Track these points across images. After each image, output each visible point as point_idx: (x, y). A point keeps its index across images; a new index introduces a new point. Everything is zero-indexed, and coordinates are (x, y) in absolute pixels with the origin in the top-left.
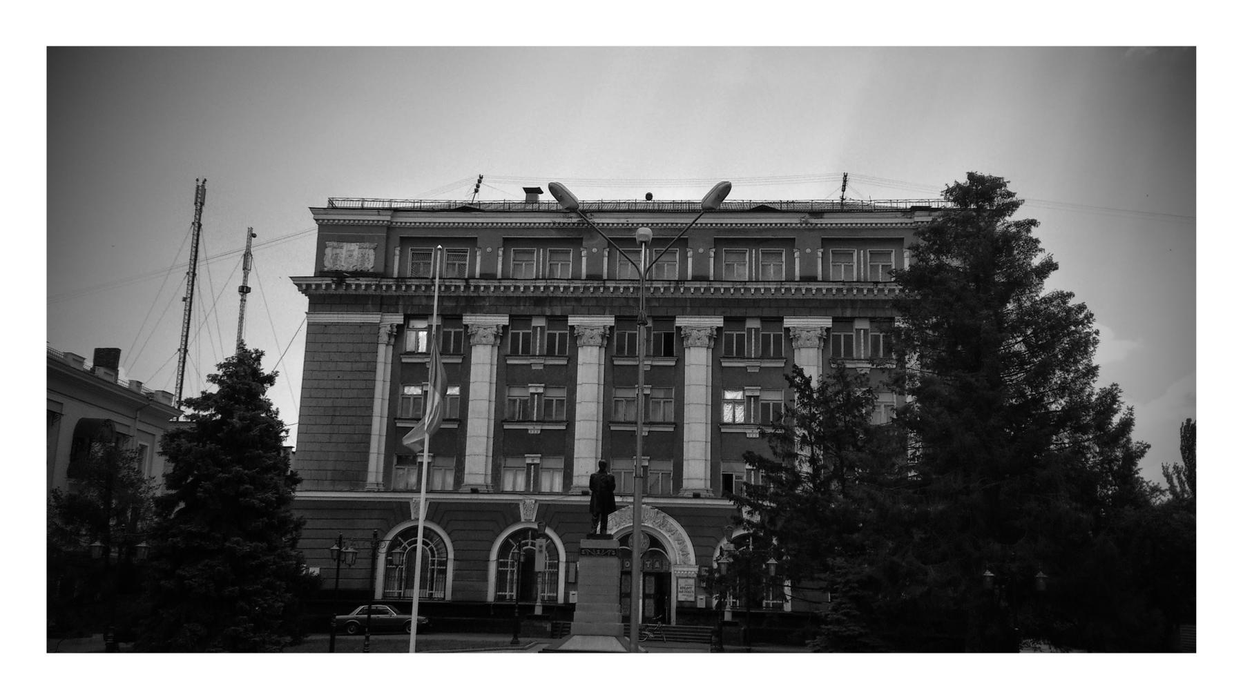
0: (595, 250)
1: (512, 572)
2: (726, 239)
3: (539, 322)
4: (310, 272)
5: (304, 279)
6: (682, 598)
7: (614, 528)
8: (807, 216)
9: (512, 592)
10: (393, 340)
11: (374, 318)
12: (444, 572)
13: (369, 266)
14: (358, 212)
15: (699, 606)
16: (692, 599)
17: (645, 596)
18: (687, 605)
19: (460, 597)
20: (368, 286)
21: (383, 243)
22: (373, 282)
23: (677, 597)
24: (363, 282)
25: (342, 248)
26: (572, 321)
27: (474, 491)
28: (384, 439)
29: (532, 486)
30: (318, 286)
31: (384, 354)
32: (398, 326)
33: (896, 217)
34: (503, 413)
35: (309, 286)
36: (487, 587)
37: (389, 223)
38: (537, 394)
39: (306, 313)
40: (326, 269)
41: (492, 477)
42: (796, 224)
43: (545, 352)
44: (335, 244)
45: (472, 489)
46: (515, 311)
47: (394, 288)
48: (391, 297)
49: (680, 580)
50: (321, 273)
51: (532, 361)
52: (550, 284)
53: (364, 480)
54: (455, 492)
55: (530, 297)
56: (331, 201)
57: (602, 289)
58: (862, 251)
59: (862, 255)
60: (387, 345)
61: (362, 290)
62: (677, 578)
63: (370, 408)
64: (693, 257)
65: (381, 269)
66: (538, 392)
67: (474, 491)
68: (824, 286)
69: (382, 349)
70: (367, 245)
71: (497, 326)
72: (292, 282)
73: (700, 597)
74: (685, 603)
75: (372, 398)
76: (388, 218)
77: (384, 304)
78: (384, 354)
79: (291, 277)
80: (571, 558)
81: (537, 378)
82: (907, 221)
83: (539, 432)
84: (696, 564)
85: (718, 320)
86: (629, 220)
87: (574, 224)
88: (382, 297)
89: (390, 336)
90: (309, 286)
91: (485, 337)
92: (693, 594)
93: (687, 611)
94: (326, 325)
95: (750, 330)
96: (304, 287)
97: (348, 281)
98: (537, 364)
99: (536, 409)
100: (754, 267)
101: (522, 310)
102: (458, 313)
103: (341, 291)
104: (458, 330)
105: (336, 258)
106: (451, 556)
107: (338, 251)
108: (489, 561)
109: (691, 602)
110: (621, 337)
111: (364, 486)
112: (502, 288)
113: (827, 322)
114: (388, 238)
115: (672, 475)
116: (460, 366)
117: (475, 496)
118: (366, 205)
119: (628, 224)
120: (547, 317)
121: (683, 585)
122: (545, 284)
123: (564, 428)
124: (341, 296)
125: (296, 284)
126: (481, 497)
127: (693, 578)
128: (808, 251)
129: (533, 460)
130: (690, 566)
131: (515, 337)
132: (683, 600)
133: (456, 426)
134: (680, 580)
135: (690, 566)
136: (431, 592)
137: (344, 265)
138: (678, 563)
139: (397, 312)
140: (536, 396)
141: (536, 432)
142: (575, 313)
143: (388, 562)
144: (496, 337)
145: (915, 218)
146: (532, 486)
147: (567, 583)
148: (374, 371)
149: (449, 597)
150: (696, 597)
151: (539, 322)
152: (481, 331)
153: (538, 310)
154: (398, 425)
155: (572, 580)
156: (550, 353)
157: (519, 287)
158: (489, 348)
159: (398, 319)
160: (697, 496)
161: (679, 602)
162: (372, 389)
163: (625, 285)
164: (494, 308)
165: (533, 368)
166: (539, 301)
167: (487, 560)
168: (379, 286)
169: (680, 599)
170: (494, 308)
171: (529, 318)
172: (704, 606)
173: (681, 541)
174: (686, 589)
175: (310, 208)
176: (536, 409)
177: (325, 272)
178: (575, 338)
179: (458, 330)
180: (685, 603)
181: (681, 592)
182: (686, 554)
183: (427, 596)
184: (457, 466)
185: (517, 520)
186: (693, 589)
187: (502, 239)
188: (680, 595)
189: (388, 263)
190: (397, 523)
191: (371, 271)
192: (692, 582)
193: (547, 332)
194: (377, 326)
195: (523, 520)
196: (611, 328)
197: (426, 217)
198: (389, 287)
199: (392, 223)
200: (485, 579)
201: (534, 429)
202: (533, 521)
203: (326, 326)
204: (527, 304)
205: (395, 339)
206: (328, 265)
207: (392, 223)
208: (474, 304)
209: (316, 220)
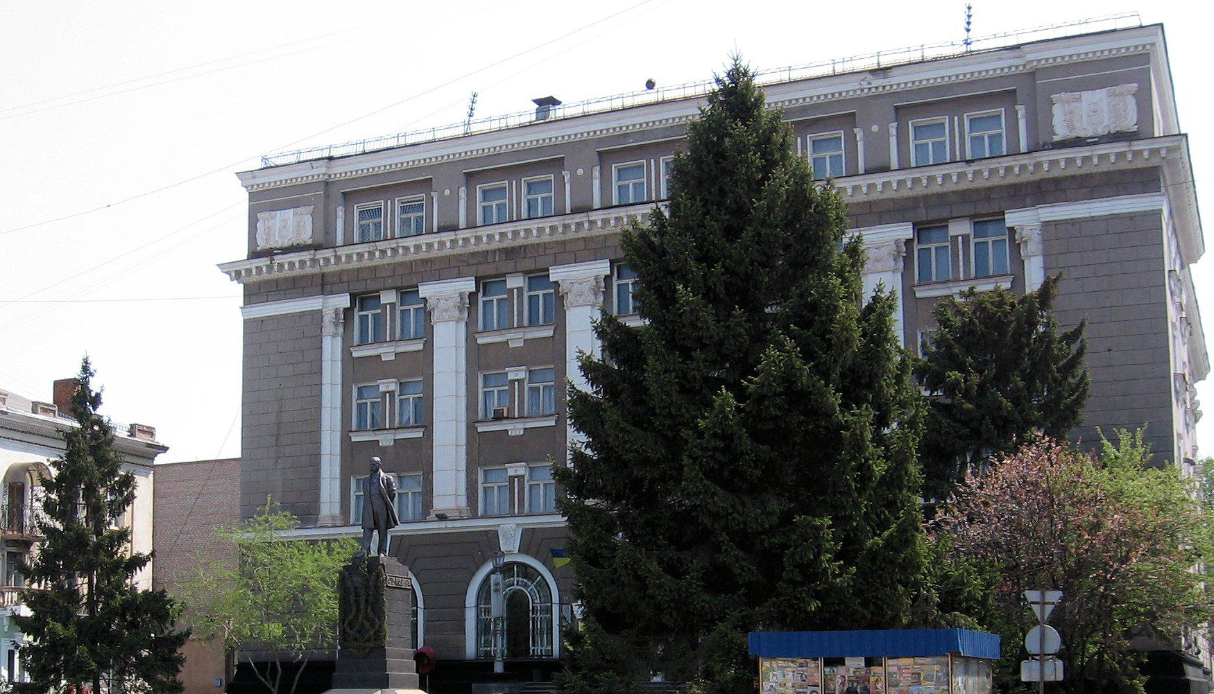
2: (922, 104)
3: (514, 282)
4: (243, 254)
5: (230, 265)
8: (869, 76)
10: (341, 330)
11: (313, 303)
13: (306, 237)
14: (463, 141)
20: (302, 263)
21: (321, 206)
22: (306, 256)
24: (295, 257)
25: (274, 217)
27: (442, 517)
28: (338, 458)
30: (249, 271)
31: (332, 348)
35: (238, 273)
37: (326, 177)
39: (241, 308)
40: (259, 249)
42: (855, 91)
43: (526, 322)
44: (266, 214)
45: (437, 516)
47: (332, 261)
48: (334, 273)
50: (254, 254)
54: (423, 520)
55: (499, 250)
56: (264, 159)
57: (586, 225)
58: (956, 118)
59: (956, 123)
60: (334, 336)
61: (298, 271)
63: (318, 420)
64: (438, 201)
65: (321, 239)
67: (442, 517)
68: (907, 176)
69: (327, 342)
70: (302, 209)
71: (461, 295)
72: (220, 270)
75: (319, 407)
76: (323, 170)
77: (323, 284)
78: (332, 348)
79: (218, 265)
81: (517, 358)
83: (522, 433)
85: (602, 266)
86: (621, 121)
88: (323, 275)
89: (336, 325)
90: (238, 273)
91: (446, 311)
94: (262, 321)
96: (233, 274)
100: (514, 199)
105: (268, 230)
107: (271, 222)
110: (363, 320)
111: (316, 520)
112: (460, 242)
113: (905, 231)
114: (327, 196)
116: (421, 354)
117: (442, 524)
118: (439, 135)
119: (621, 128)
123: (553, 423)
124: (277, 281)
125: (226, 273)
126: (450, 524)
128: (875, 128)
137: (278, 241)
141: (517, 434)
144: (461, 311)
145: (1027, 56)
148: (320, 372)
151: (514, 282)
153: (510, 266)
158: (453, 324)
159: (344, 301)
162: (318, 397)
163: (617, 215)
164: (456, 271)
166: (510, 253)
168: (314, 261)
170: (456, 271)
171: (501, 276)
175: (237, 173)
177: (259, 252)
178: (560, 299)
187: (463, 176)
189: (329, 229)
191: (310, 242)
194: (317, 315)
196: (608, 279)
197: (368, 161)
198: (327, 260)
199: (330, 175)
201: (515, 429)
202: (516, 551)
203: (262, 321)
206: (262, 244)
207: (330, 175)
209: (246, 187)
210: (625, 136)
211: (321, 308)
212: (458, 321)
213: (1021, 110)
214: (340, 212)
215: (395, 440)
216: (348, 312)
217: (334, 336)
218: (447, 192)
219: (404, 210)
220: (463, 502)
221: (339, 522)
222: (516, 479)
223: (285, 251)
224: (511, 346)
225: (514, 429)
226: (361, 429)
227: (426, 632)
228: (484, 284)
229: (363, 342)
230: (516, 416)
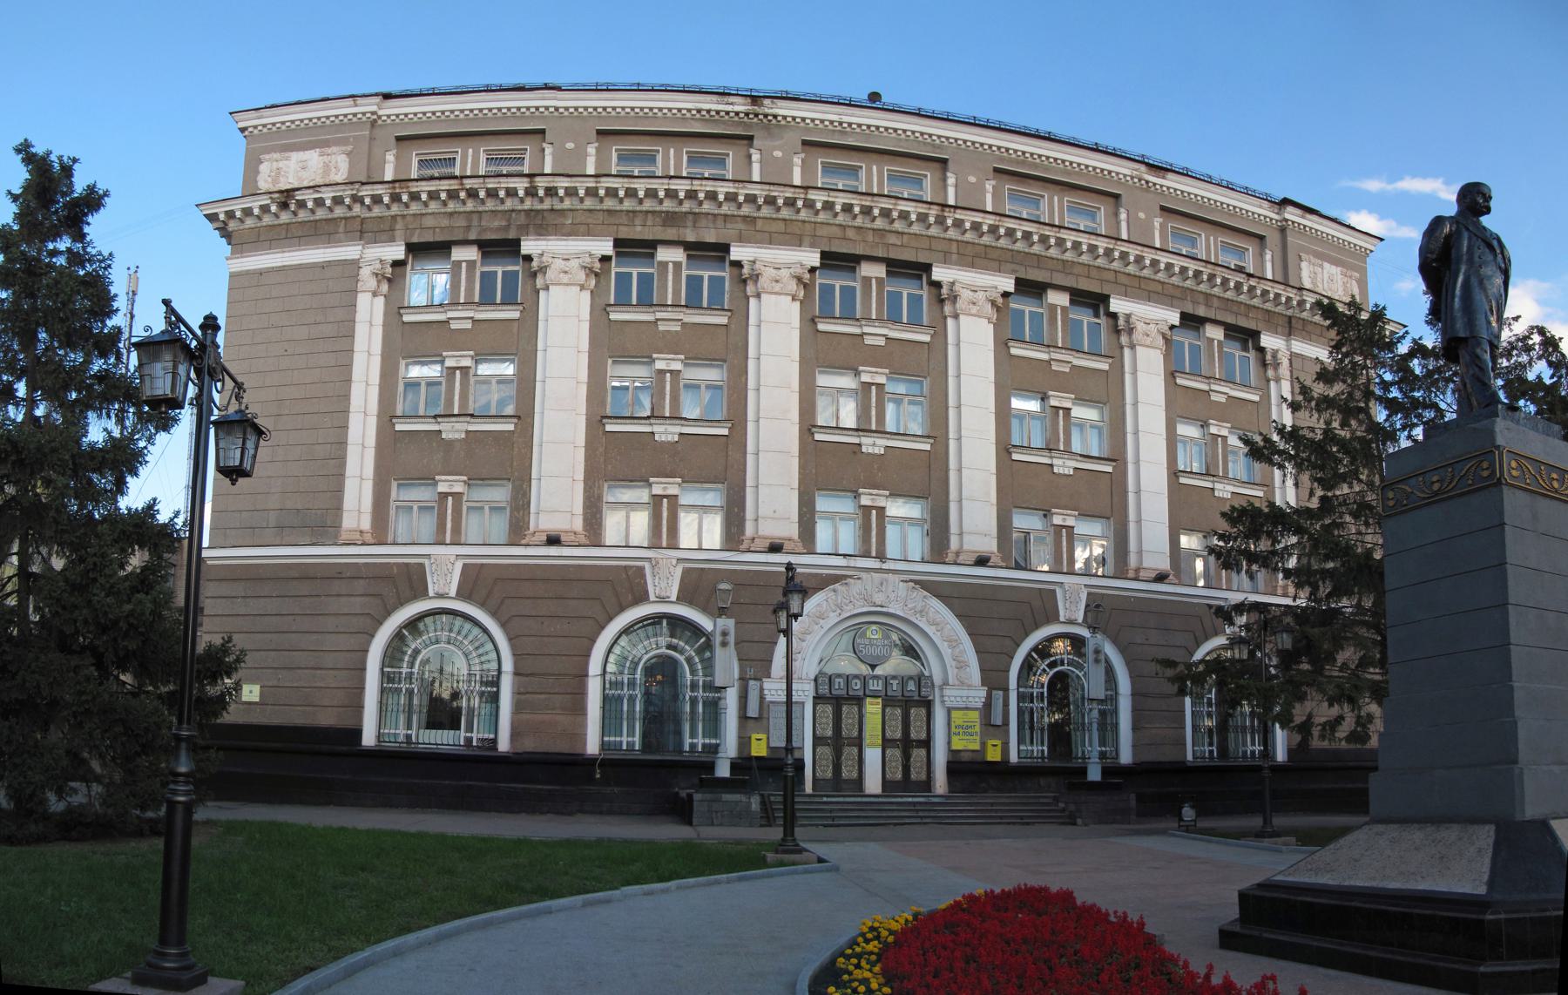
1: (632, 699)
6: (958, 744)
7: (832, 614)
9: (634, 736)
12: (495, 698)
15: (989, 758)
16: (977, 747)
17: (886, 743)
18: (965, 757)
19: (529, 745)
23: (949, 743)
26: (736, 253)
27: (553, 541)
34: (603, 403)
36: (584, 726)
38: (671, 372)
41: (585, 520)
46: (625, 233)
49: (954, 714)
51: (659, 315)
52: (698, 188)
62: (949, 711)
66: (671, 368)
67: (553, 541)
74: (962, 754)
80: (750, 673)
81: (671, 344)
84: (983, 685)
92: (978, 738)
93: (965, 770)
98: (670, 321)
99: (668, 397)
101: (639, 232)
102: (512, 235)
104: (510, 268)
106: (508, 666)
108: (587, 676)
109: (973, 751)
117: (553, 551)
120: (688, 246)
121: (959, 722)
122: (688, 188)
127: (976, 709)
129: (665, 489)
130: (970, 686)
131: (623, 279)
132: (960, 748)
133: (511, 427)
135: (970, 686)
136: (469, 735)
138: (951, 683)
141: (670, 438)
143: (386, 677)
147: (743, 717)
149: (504, 745)
150: (983, 744)
152: (558, 264)
154: (398, 427)
155: (753, 711)
160: (982, 561)
161: (953, 754)
165: (661, 328)
166: (670, 219)
167: (584, 675)
169: (954, 747)
171: (652, 245)
173: (953, 643)
174: (966, 729)
176: (668, 397)
179: (510, 268)
180: (962, 754)
182: (961, 665)
183: (462, 743)
184: (514, 498)
185: (641, 597)
186: (977, 729)
188: (955, 739)
190: (401, 603)
192: (975, 716)
193: (684, 273)
195: (652, 598)
200: (580, 709)
202: (674, 598)
204: (649, 223)
215: (468, 432)
220: (578, 524)
221: (368, 538)
222: (665, 500)
224: (661, 328)
225: (666, 433)
227: (518, 708)
228: (629, 248)
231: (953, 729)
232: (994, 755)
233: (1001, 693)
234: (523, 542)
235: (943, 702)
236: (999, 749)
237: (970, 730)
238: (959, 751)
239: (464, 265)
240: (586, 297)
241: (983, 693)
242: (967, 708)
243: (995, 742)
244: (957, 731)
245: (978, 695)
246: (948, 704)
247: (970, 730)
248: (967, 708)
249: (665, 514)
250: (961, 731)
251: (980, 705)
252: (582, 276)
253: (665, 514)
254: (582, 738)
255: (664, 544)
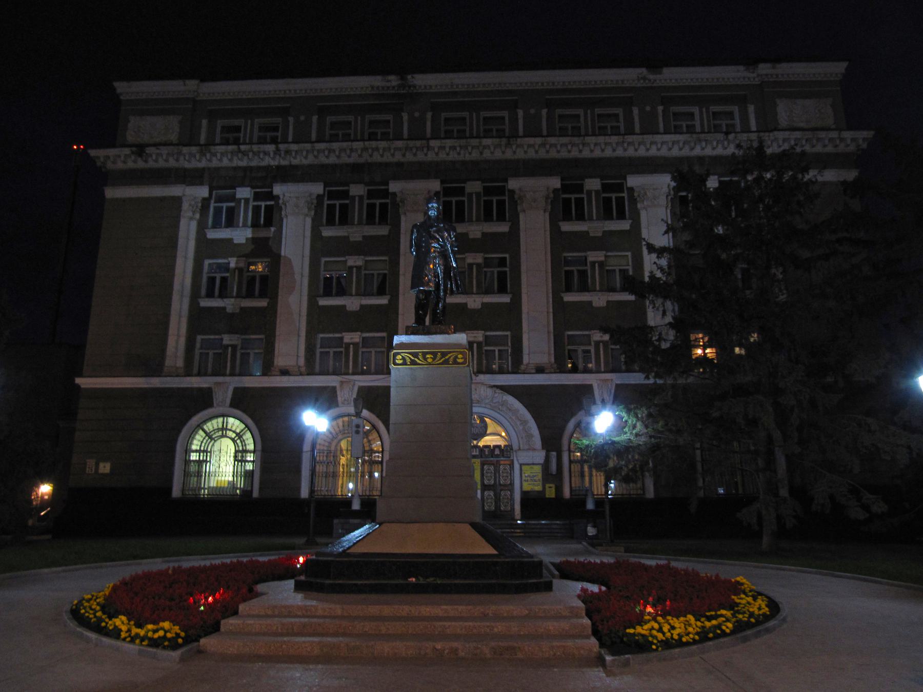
0: (417, 114)
3: (357, 190)
6: (527, 487)
16: (538, 488)
29: (351, 367)
32: (204, 199)
33: (738, 71)
38: (356, 267)
48: (196, 170)
49: (524, 468)
53: (161, 364)
62: (521, 465)
69: (183, 223)
71: (311, 195)
73: (547, 485)
82: (752, 75)
87: (394, 87)
92: (541, 483)
93: (532, 503)
95: (589, 193)
97: (149, 150)
103: (141, 164)
109: (538, 492)
115: (510, 351)
134: (524, 468)
135: (534, 450)
139: (201, 184)
140: (355, 269)
142: (396, 178)
144: (309, 209)
146: (351, 367)
156: (370, 221)
157: (334, 151)
166: (356, 168)
172: (553, 496)
181: (525, 481)
182: (530, 436)
192: (538, 469)
205: (201, 215)
208: (286, 174)
210: (455, 94)
211: (180, 194)
212: (307, 215)
213: (751, 109)
214: (204, 122)
216: (205, 202)
217: (191, 219)
218: (302, 118)
219: (261, 129)
220: (302, 361)
223: (155, 145)
226: (210, 295)
229: (216, 225)
230: (354, 293)
231: (524, 478)
232: (551, 493)
233: (554, 453)
234: (269, 374)
235: (518, 460)
236: (553, 490)
237: (535, 478)
238: (528, 492)
239: (243, 201)
240: (309, 221)
241: (543, 454)
242: (533, 464)
243: (551, 485)
244: (526, 479)
245: (540, 456)
246: (521, 462)
247: (535, 478)
248: (533, 464)
249: (351, 354)
250: (529, 478)
251: (542, 461)
252: (306, 211)
253: (351, 354)
254: (299, 489)
255: (351, 371)
